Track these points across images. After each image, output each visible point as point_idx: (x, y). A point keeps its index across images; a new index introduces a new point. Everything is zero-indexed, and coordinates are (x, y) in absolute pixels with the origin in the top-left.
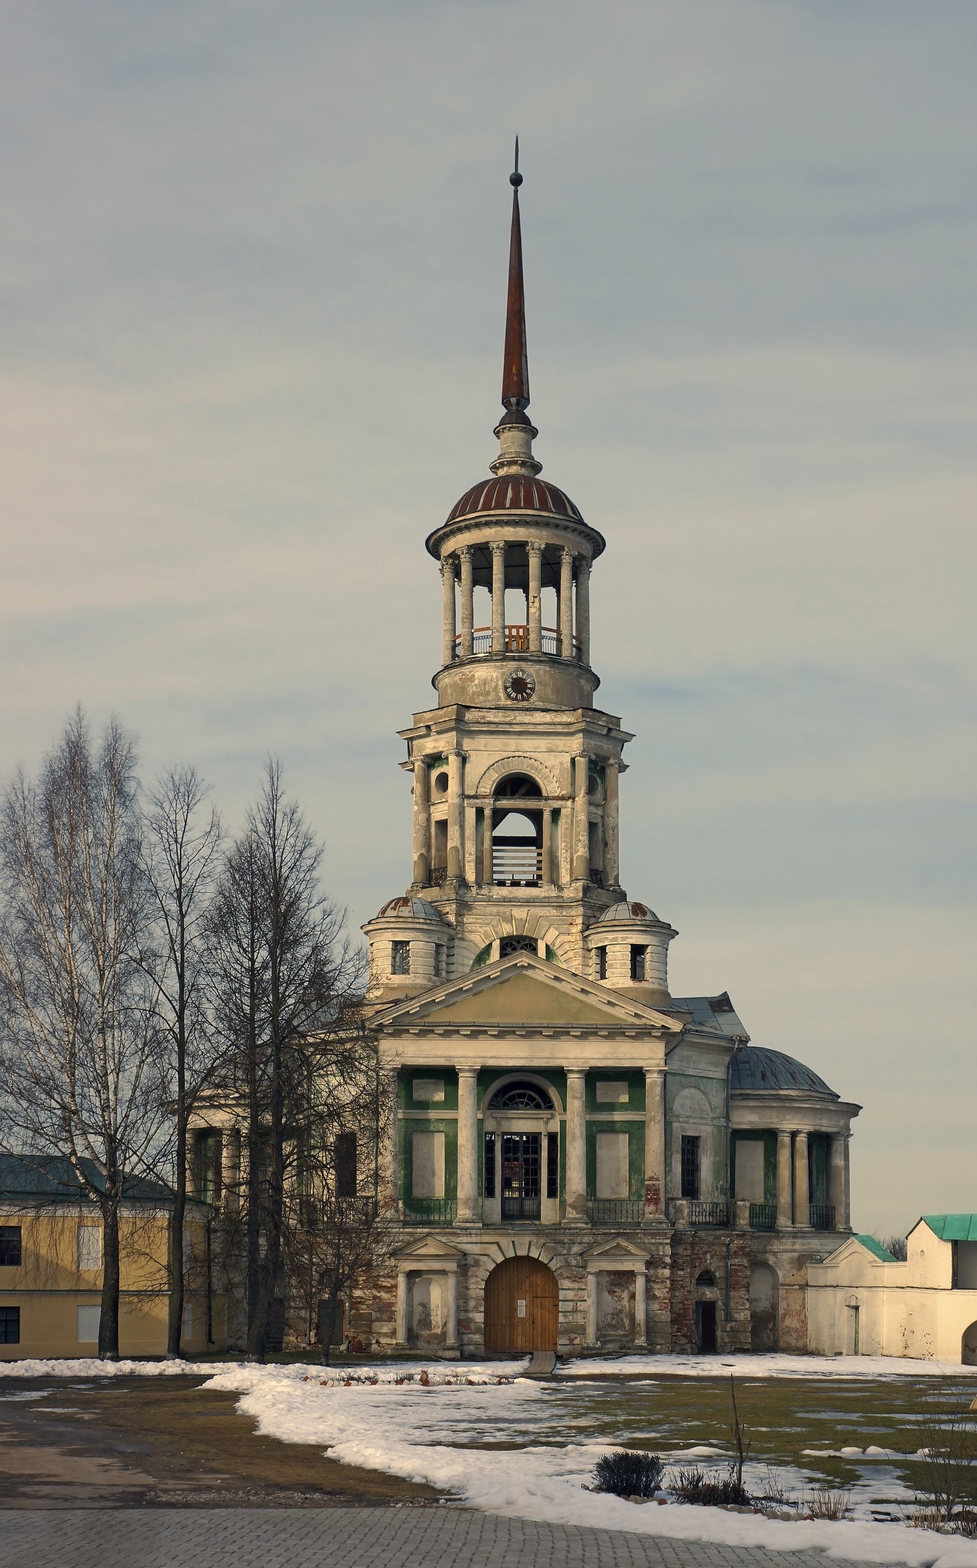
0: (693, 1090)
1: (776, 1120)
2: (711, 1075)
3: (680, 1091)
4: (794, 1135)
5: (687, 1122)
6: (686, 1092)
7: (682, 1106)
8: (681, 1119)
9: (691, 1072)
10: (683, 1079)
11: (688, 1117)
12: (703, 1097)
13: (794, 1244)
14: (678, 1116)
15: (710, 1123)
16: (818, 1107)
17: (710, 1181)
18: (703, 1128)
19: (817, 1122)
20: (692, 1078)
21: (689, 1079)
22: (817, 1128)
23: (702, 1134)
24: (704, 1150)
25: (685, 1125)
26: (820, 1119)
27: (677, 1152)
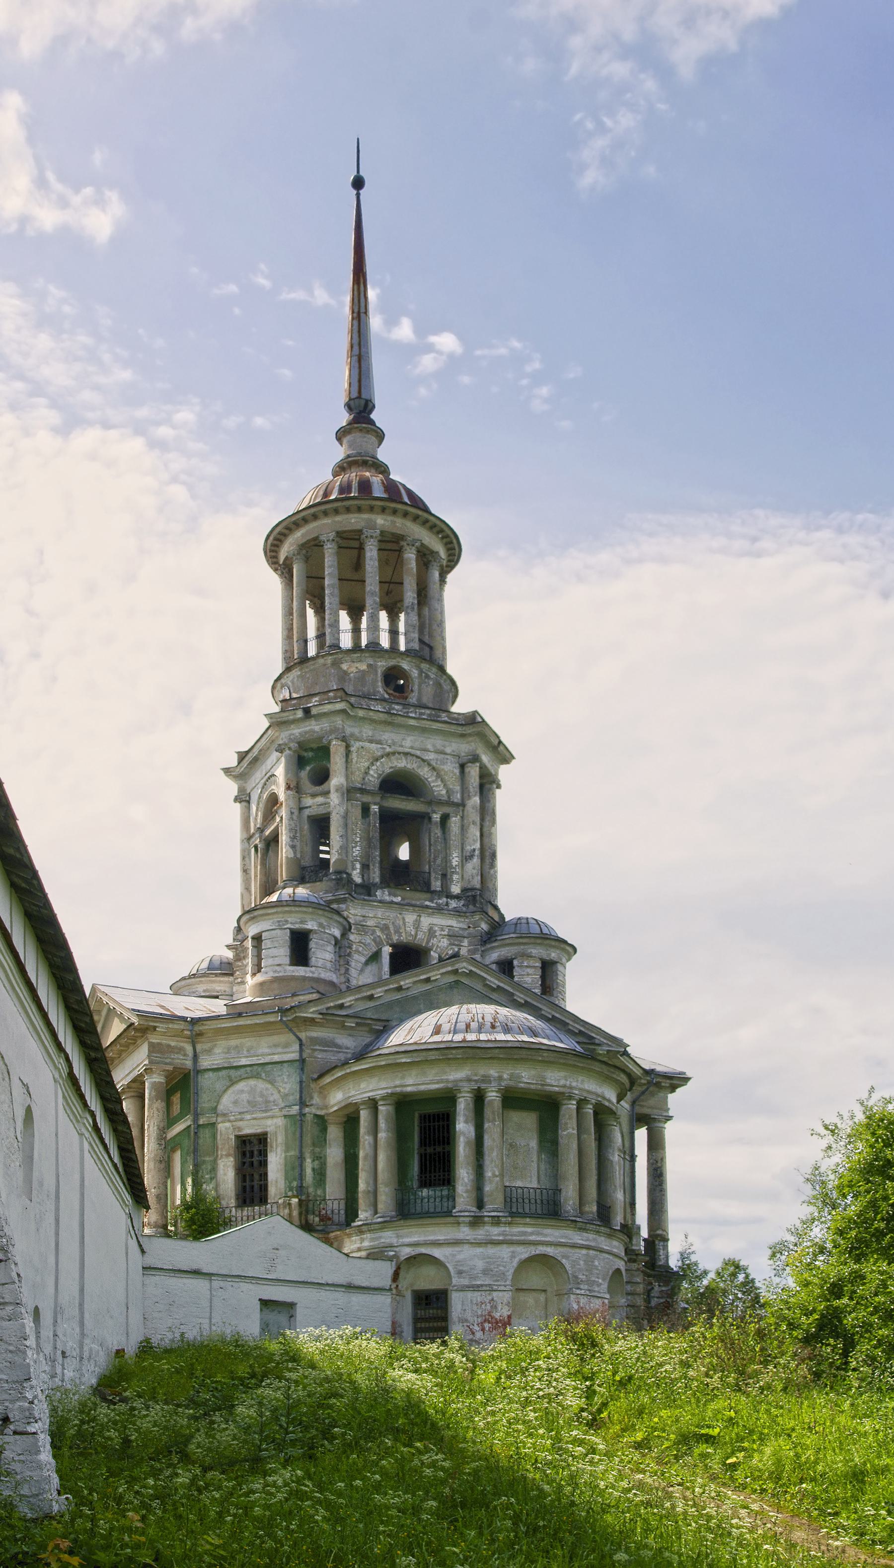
0: (252, 1082)
1: (353, 1093)
2: (276, 1058)
3: (228, 1087)
4: (373, 1104)
5: (241, 1120)
6: (241, 1085)
7: (235, 1102)
8: (232, 1118)
9: (244, 1062)
10: (233, 1073)
11: (240, 1113)
12: (269, 1086)
13: (362, 1240)
14: (224, 1115)
15: (279, 1114)
16: (383, 1063)
17: (282, 1184)
18: (269, 1122)
19: (398, 1082)
20: (248, 1069)
21: (243, 1070)
22: (398, 1090)
23: (268, 1129)
24: (272, 1147)
25: (240, 1124)
26: (403, 1078)
27: (228, 1155)
